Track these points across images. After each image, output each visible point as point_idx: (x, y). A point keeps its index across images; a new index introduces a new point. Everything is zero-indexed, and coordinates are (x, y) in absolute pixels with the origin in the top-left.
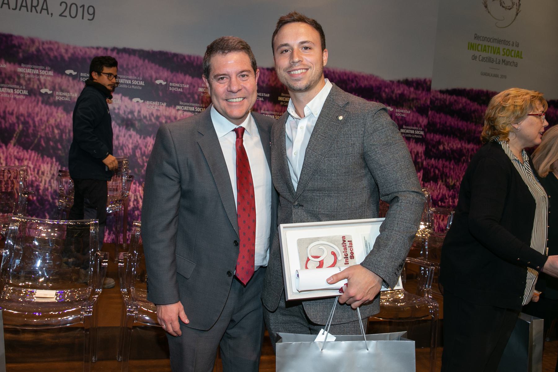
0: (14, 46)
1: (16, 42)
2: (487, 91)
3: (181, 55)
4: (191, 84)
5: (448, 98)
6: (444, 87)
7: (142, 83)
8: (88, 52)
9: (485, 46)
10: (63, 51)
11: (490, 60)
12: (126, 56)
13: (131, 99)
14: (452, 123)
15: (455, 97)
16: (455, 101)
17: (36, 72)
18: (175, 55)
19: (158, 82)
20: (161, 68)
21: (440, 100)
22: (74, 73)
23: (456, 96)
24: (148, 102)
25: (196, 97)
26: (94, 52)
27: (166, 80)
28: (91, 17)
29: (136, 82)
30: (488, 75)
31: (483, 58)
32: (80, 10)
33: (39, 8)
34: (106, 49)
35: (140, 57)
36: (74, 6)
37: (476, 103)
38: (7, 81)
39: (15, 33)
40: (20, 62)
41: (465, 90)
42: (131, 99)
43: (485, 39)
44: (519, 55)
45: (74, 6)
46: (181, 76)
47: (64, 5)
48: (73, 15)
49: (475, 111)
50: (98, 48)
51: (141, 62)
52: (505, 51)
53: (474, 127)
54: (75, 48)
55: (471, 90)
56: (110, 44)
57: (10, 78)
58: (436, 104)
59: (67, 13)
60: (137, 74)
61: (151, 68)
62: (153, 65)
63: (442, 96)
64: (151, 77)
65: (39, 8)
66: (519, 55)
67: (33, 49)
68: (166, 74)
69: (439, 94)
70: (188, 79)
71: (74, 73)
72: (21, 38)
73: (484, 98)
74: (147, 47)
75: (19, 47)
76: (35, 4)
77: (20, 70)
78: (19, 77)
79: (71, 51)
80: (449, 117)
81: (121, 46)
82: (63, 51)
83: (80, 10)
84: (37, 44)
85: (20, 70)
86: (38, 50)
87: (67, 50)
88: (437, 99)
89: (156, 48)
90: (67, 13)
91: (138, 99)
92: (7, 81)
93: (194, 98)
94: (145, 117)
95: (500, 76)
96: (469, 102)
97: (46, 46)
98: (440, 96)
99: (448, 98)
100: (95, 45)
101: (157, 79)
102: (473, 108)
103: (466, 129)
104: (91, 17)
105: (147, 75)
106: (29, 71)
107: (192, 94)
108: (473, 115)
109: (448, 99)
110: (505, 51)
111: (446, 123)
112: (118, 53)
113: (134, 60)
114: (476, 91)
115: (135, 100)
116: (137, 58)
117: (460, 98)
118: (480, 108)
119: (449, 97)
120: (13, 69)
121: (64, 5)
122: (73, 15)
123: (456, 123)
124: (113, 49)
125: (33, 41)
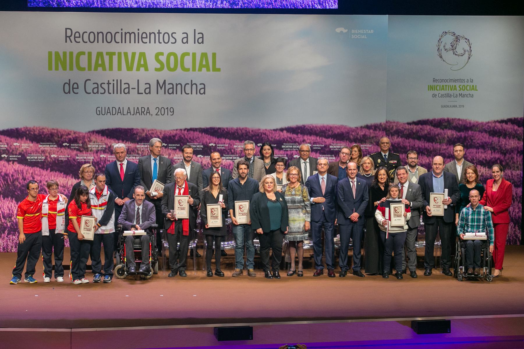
0: (134, 134)
1: (135, 132)
2: (448, 119)
3: (223, 128)
4: (229, 144)
5: (415, 128)
6: (410, 121)
7: (202, 146)
8: (172, 133)
9: (443, 86)
10: (159, 134)
11: (449, 96)
12: (192, 132)
13: (196, 155)
14: (420, 145)
15: (420, 126)
16: (421, 129)
17: (146, 146)
18: (219, 128)
19: (211, 145)
20: (212, 137)
21: (408, 129)
22: (166, 145)
23: (422, 125)
24: (206, 157)
25: (233, 151)
26: (175, 132)
27: (215, 143)
28: (172, 113)
29: (198, 146)
30: (448, 106)
31: (442, 95)
32: (166, 110)
33: (145, 113)
34: (181, 130)
35: (200, 132)
36: (163, 109)
37: (439, 128)
38: (132, 153)
39: (134, 127)
40: (138, 142)
41: (428, 120)
42: (196, 155)
43: (446, 81)
44: (474, 88)
45: (163, 109)
46: (223, 140)
47: (158, 109)
48: (163, 114)
49: (438, 135)
50: (177, 130)
51: (200, 135)
52: (461, 87)
53: (439, 146)
54: (165, 131)
55: (434, 120)
56: (183, 127)
57: (133, 151)
58: (405, 133)
59: (159, 113)
60: (199, 141)
61: (206, 137)
62: (207, 135)
63: (410, 127)
64: (207, 142)
65: (145, 113)
66: (474, 88)
67: (144, 135)
68: (215, 139)
69: (407, 125)
70: (227, 141)
71: (166, 145)
72: (137, 129)
73: (446, 124)
74: (203, 126)
75: (137, 134)
76: (143, 111)
77: (138, 146)
78: (138, 150)
79: (163, 133)
80: (416, 141)
81: (189, 127)
82: (159, 134)
83: (166, 110)
84: (145, 132)
85: (138, 146)
86: (146, 135)
87: (161, 133)
88: (405, 129)
89: (208, 126)
90: (159, 113)
91: (201, 156)
92: (132, 153)
93: (231, 152)
94: (205, 165)
95: (458, 106)
96: (433, 128)
97: (150, 132)
98: (407, 127)
99: (415, 128)
100: (175, 128)
101: (210, 143)
102: (436, 133)
103: (432, 149)
104: (172, 113)
105: (204, 142)
106: (142, 146)
107: (230, 150)
108: (437, 137)
109: (414, 128)
110: (461, 87)
111: (414, 145)
112: (188, 131)
113: (197, 134)
114: (438, 120)
115: (199, 156)
116: (198, 133)
117: (425, 126)
118: (442, 131)
119: (415, 127)
120: (134, 146)
121: (158, 109)
122: (163, 114)
123: (423, 145)
124: (185, 130)
125: (143, 130)
